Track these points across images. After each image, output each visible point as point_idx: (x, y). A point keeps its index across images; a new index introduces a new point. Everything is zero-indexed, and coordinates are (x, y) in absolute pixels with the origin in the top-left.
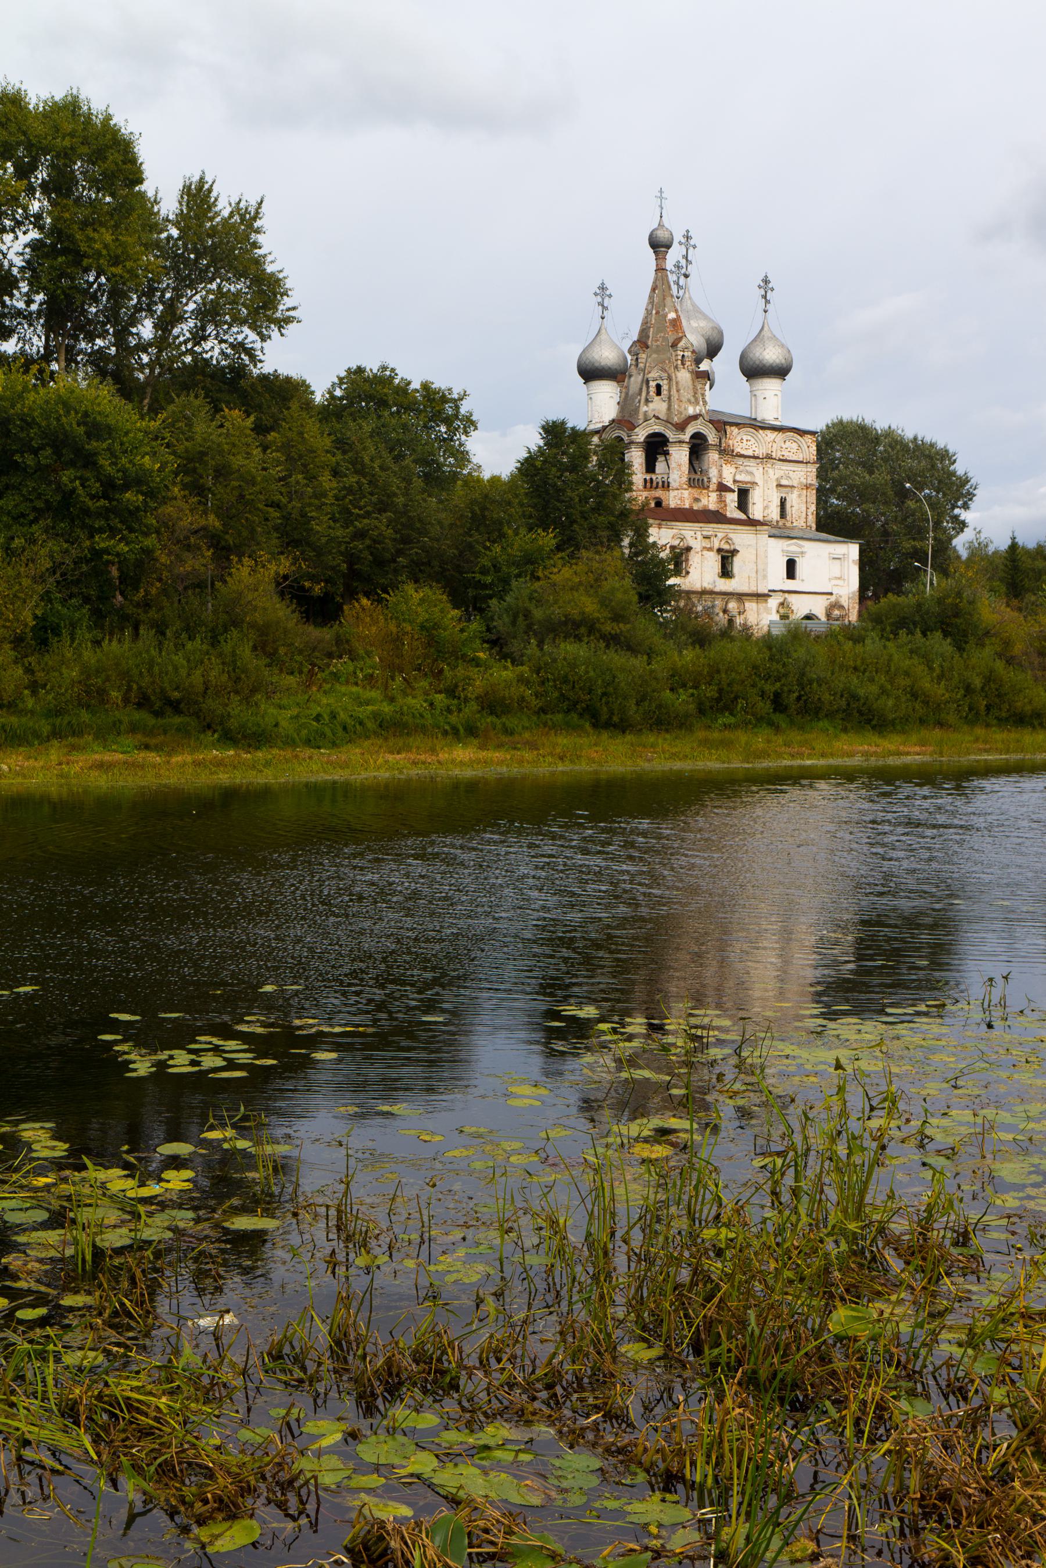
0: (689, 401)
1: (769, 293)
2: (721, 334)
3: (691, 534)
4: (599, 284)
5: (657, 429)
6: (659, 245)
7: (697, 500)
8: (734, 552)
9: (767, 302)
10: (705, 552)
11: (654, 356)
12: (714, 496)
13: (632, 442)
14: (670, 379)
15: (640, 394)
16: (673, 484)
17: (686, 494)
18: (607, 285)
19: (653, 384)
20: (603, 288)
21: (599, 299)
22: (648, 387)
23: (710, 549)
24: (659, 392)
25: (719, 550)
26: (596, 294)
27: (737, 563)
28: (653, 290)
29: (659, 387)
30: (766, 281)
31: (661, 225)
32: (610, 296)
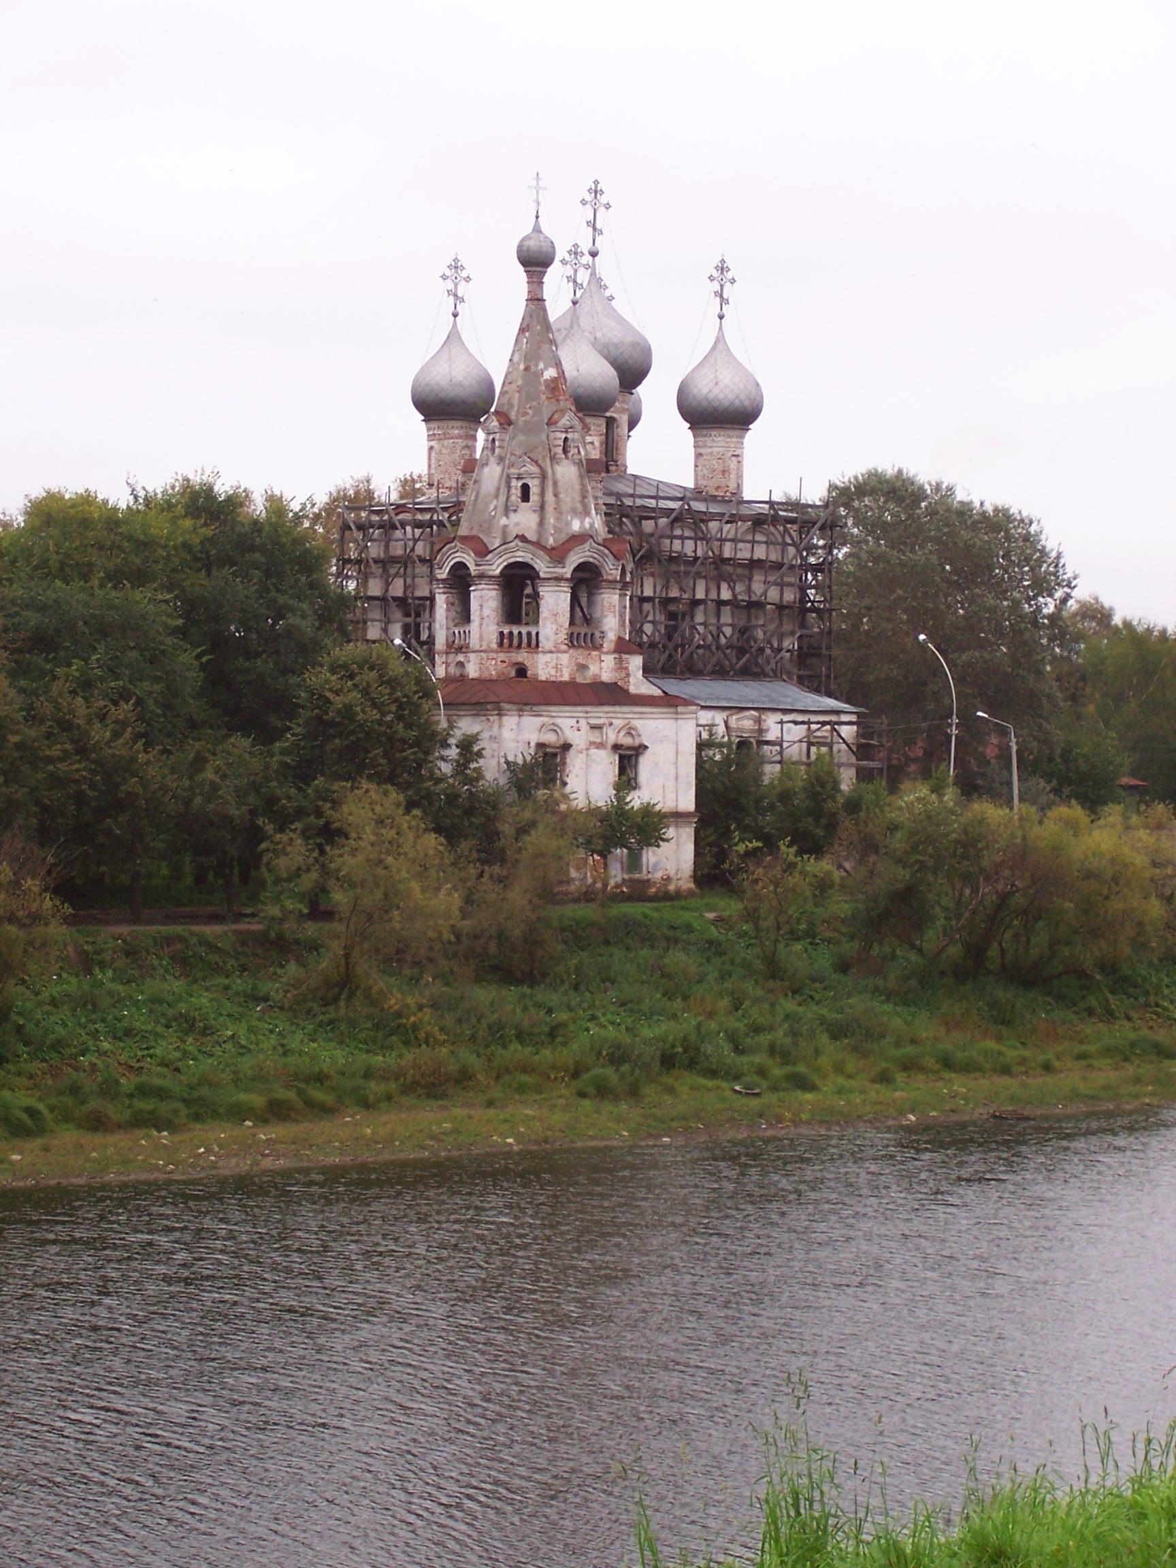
0: (574, 512)
1: (727, 286)
2: (647, 353)
3: (571, 725)
4: (449, 261)
5: (522, 556)
6: (535, 262)
7: (582, 667)
8: (641, 749)
9: (724, 301)
10: (593, 751)
11: (521, 437)
12: (609, 661)
13: (481, 576)
14: (543, 477)
15: (496, 497)
16: (545, 644)
17: (565, 658)
18: (463, 261)
19: (516, 485)
20: (456, 266)
21: (451, 286)
22: (509, 487)
23: (601, 746)
24: (525, 496)
25: (616, 747)
26: (444, 277)
27: (645, 766)
28: (522, 330)
29: (525, 489)
30: (722, 268)
31: (537, 229)
32: (468, 279)
